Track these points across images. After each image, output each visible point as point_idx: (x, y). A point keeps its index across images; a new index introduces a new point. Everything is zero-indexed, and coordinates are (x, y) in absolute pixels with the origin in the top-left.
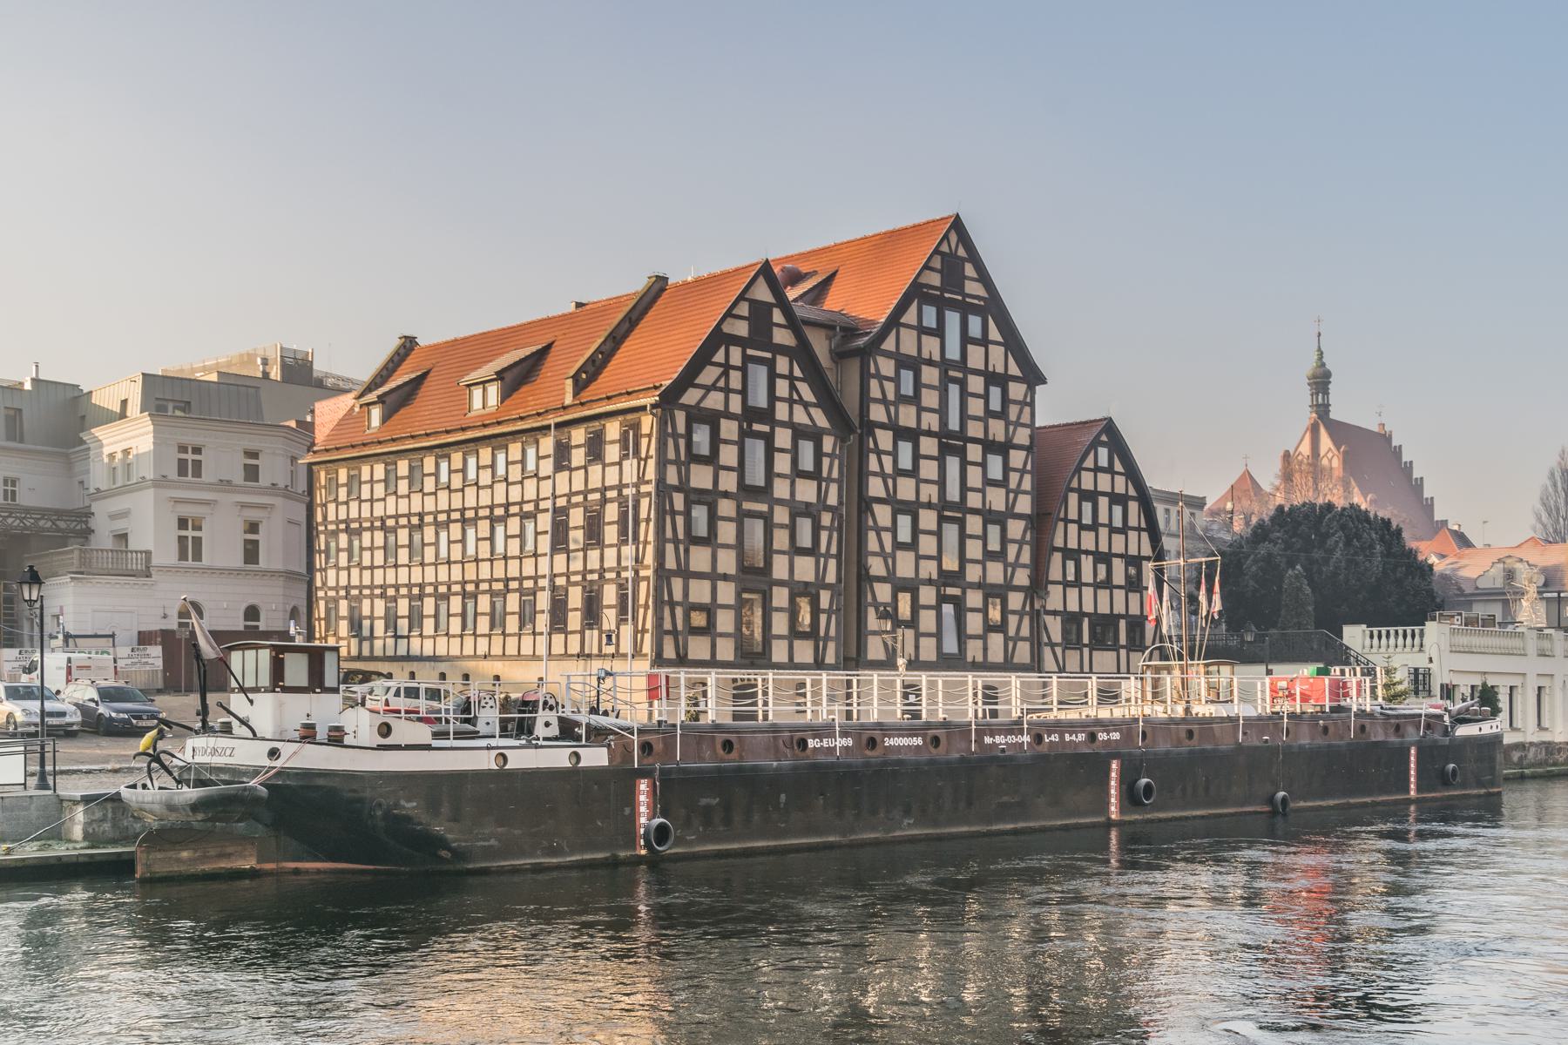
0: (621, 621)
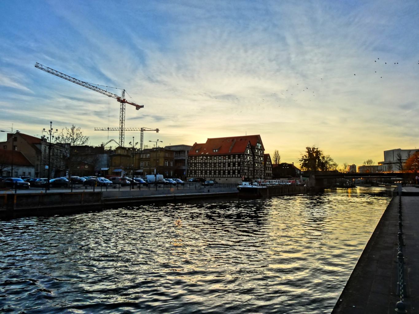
0: (238, 174)
